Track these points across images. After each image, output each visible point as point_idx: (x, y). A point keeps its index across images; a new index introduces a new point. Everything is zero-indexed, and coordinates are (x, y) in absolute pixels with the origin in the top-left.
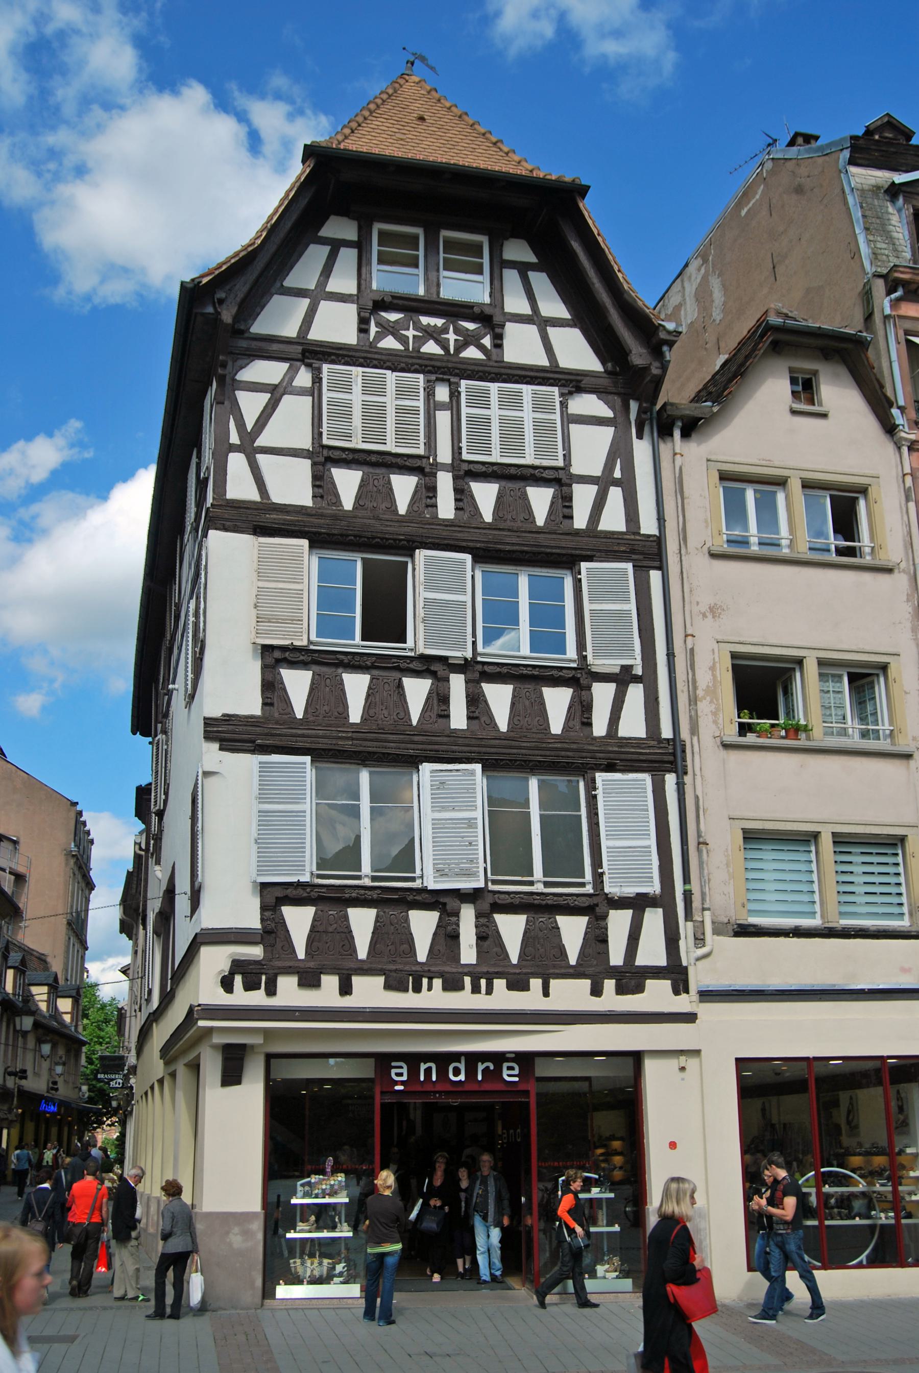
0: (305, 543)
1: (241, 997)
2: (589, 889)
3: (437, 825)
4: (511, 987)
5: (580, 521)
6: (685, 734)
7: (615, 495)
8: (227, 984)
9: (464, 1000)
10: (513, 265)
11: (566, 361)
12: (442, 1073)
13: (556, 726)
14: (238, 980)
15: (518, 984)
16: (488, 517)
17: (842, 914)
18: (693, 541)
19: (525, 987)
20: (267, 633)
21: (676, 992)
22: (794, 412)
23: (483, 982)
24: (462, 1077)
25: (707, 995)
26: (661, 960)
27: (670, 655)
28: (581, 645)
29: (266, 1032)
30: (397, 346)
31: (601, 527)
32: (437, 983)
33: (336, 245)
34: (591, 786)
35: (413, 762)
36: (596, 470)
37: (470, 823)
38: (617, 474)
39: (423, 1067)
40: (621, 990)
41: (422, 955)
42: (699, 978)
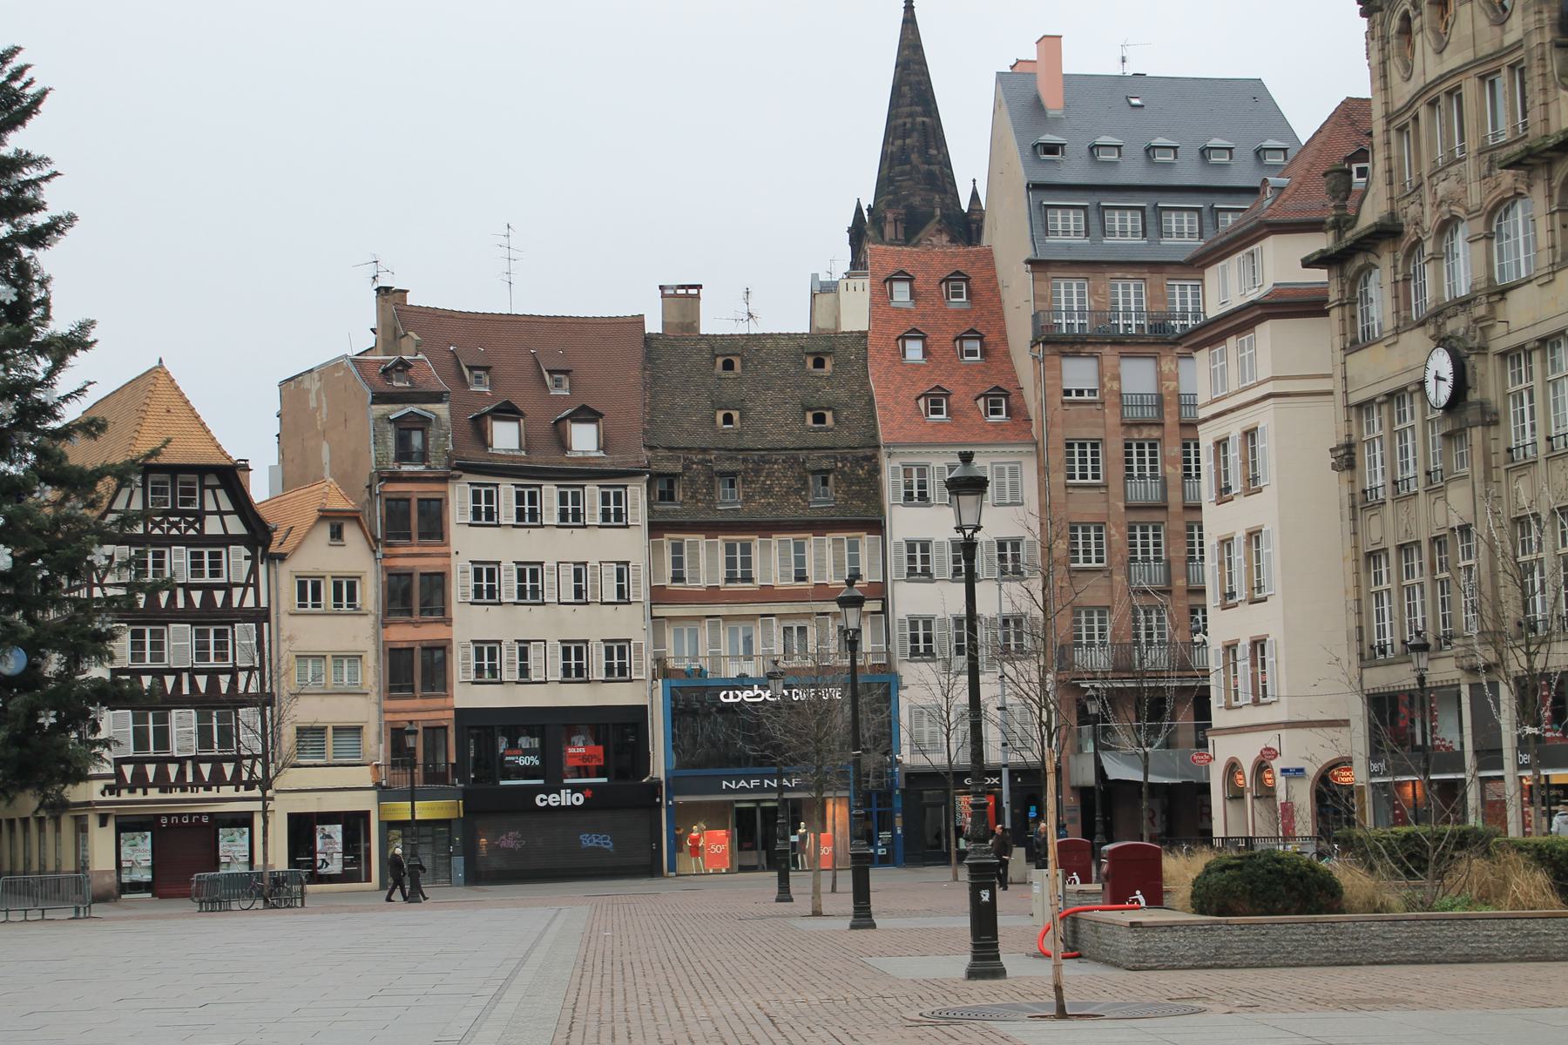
1: (108, 798)
2: (235, 753)
5: (235, 604)
6: (275, 690)
7: (251, 590)
8: (103, 793)
9: (188, 795)
12: (180, 820)
13: (224, 691)
15: (208, 788)
16: (198, 606)
17: (335, 757)
18: (282, 610)
19: (210, 790)
22: (330, 545)
25: (277, 791)
27: (270, 660)
28: (234, 658)
30: (161, 533)
32: (178, 790)
34: (237, 714)
37: (191, 732)
38: (252, 582)
40: (246, 790)
41: (173, 780)
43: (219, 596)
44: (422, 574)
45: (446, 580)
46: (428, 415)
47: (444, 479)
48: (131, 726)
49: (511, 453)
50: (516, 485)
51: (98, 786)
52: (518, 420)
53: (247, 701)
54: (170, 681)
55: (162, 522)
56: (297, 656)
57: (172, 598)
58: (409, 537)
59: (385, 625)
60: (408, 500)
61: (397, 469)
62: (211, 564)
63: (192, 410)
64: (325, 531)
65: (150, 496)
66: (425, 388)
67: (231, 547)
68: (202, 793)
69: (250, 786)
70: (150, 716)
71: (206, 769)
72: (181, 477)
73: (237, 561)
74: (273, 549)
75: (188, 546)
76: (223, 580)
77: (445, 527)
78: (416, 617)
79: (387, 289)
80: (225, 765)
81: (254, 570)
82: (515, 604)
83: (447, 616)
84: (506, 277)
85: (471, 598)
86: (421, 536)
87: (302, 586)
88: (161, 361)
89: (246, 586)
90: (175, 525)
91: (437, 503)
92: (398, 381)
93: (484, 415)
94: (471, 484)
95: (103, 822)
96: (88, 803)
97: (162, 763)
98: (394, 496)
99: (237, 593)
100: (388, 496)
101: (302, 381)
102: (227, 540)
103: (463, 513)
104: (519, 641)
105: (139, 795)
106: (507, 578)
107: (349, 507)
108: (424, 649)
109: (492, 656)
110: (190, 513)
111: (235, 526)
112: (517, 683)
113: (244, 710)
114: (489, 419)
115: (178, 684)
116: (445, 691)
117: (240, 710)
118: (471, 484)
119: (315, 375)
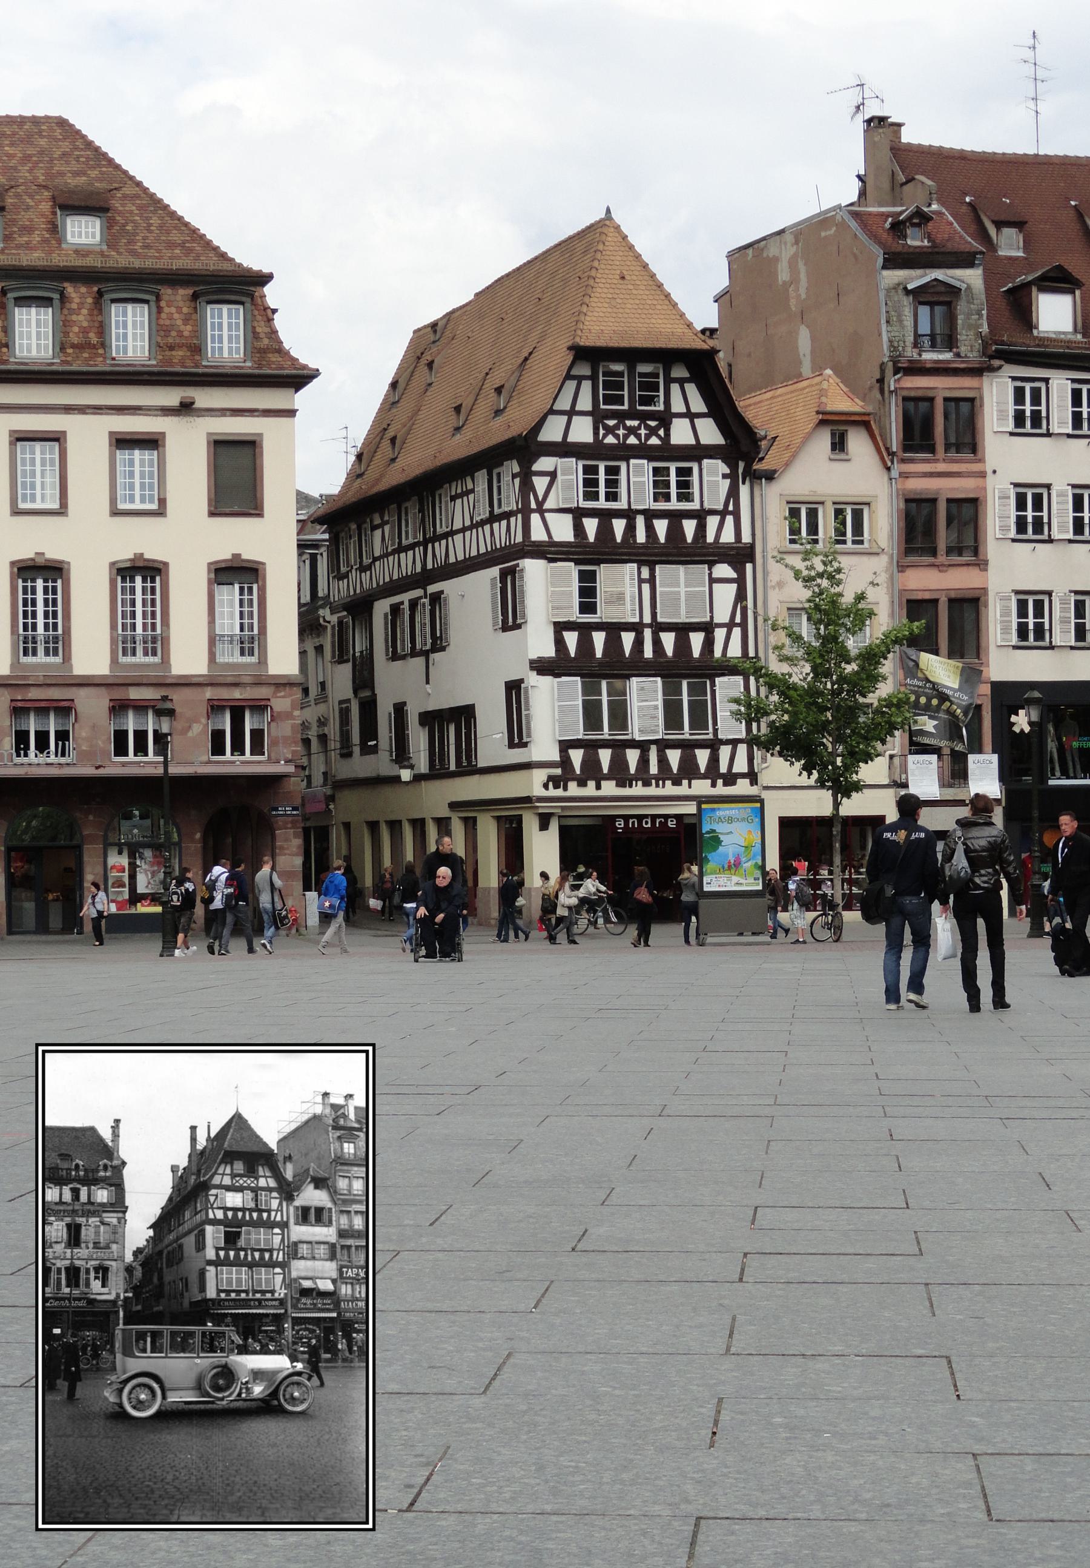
0: (572, 564)
1: (552, 792)
2: (711, 736)
3: (640, 708)
4: (673, 784)
5: (710, 539)
6: (761, 654)
7: (730, 519)
8: (546, 786)
9: (652, 791)
10: (676, 380)
11: (704, 441)
12: (640, 823)
13: (696, 653)
14: (551, 784)
15: (677, 782)
16: (662, 540)
20: (557, 615)
21: (752, 785)
22: (831, 460)
23: (661, 782)
24: (649, 825)
26: (745, 770)
29: (563, 808)
31: (721, 541)
32: (640, 783)
33: (580, 379)
34: (713, 684)
35: (628, 677)
36: (726, 619)
37: (656, 707)
38: (731, 508)
39: (631, 821)
40: (725, 784)
41: (632, 770)
42: (764, 779)
43: (689, 527)
44: (949, 501)
45: (980, 508)
46: (957, 284)
47: (977, 372)
48: (580, 699)
49: (1062, 336)
50: (1073, 381)
51: (540, 776)
52: (1072, 292)
53: (728, 668)
54: (628, 639)
55: (616, 427)
56: (789, 609)
57: (631, 529)
58: (932, 449)
59: (902, 568)
60: (931, 400)
61: (916, 356)
62: (667, 485)
63: (653, 276)
64: (824, 441)
65: (601, 392)
66: (950, 247)
67: (705, 462)
68: (670, 789)
69: (730, 779)
70: (604, 684)
71: (674, 757)
74: (755, 467)
75: (650, 459)
76: (695, 505)
77: (978, 437)
78: (942, 558)
79: (882, 120)
80: (698, 752)
82: (1070, 541)
83: (981, 557)
84: (1032, 104)
85: (1012, 534)
86: (948, 447)
87: (794, 513)
88: (608, 211)
89: (723, 514)
90: (632, 431)
91: (968, 404)
92: (913, 239)
93: (1026, 286)
94: (1014, 379)
95: (544, 826)
96: (528, 800)
97: (619, 747)
98: (913, 394)
99: (712, 522)
100: (906, 393)
101: (766, 246)
102: (698, 452)
103: (1002, 417)
104: (1076, 593)
105: (590, 790)
106: (1061, 507)
107: (857, 409)
108: (951, 601)
109: (1039, 613)
110: (652, 416)
111: (710, 433)
112: (1072, 648)
113: (725, 679)
114: (1034, 289)
115: (639, 643)
116: (978, 657)
117: (717, 680)
118: (1014, 379)
119: (789, 238)
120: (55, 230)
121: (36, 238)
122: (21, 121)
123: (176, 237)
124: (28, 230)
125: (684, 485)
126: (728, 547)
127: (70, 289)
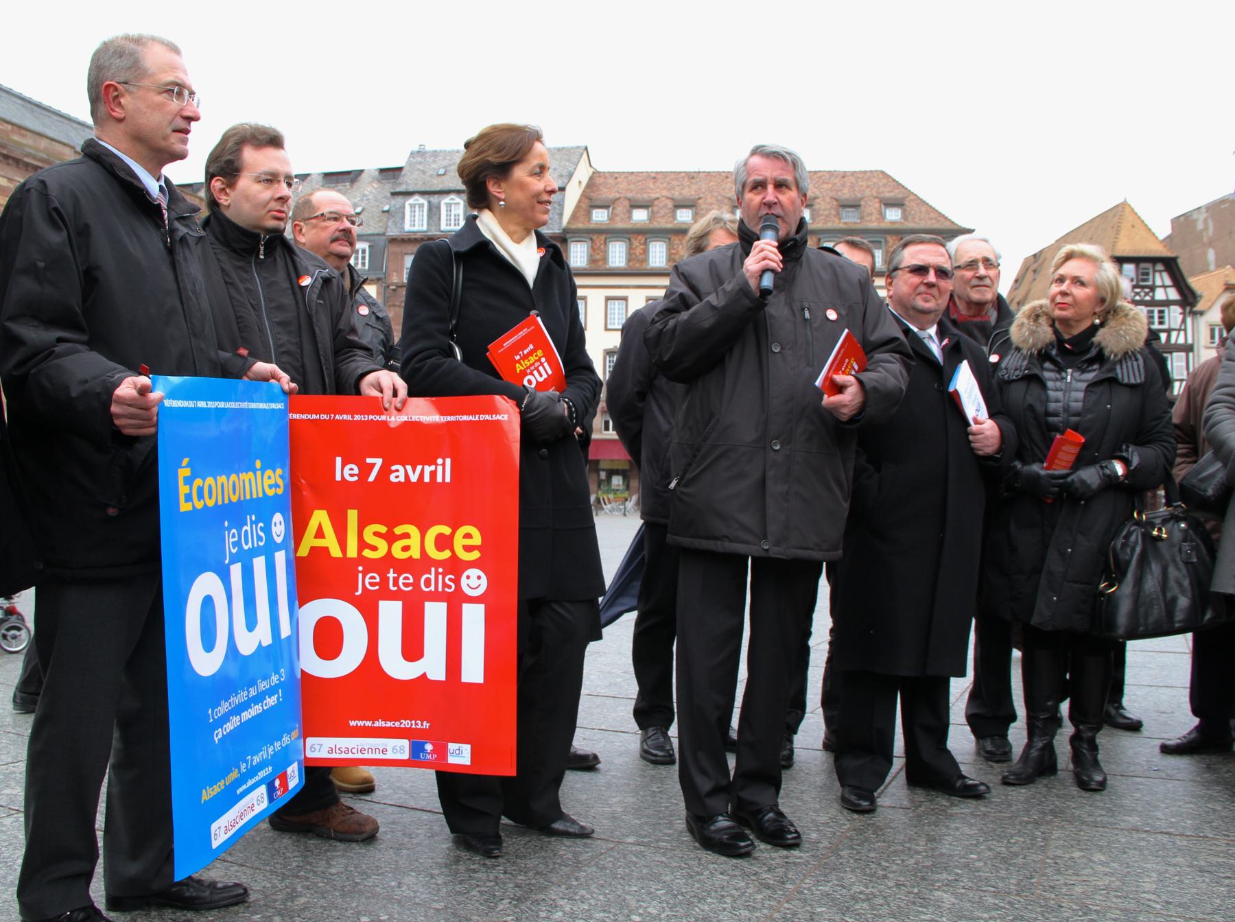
7: (1182, 333)
72: (1143, 265)
73: (1174, 315)
81: (1184, 321)
89: (1179, 330)
99: (1174, 334)
101: (1190, 216)
102: (1168, 303)
110: (1147, 287)
111: (1173, 294)
119: (1203, 210)
120: (882, 216)
121: (874, 218)
122: (865, 172)
123: (932, 215)
124: (871, 214)
125: (1161, 317)
126: (1181, 345)
127: (889, 238)
